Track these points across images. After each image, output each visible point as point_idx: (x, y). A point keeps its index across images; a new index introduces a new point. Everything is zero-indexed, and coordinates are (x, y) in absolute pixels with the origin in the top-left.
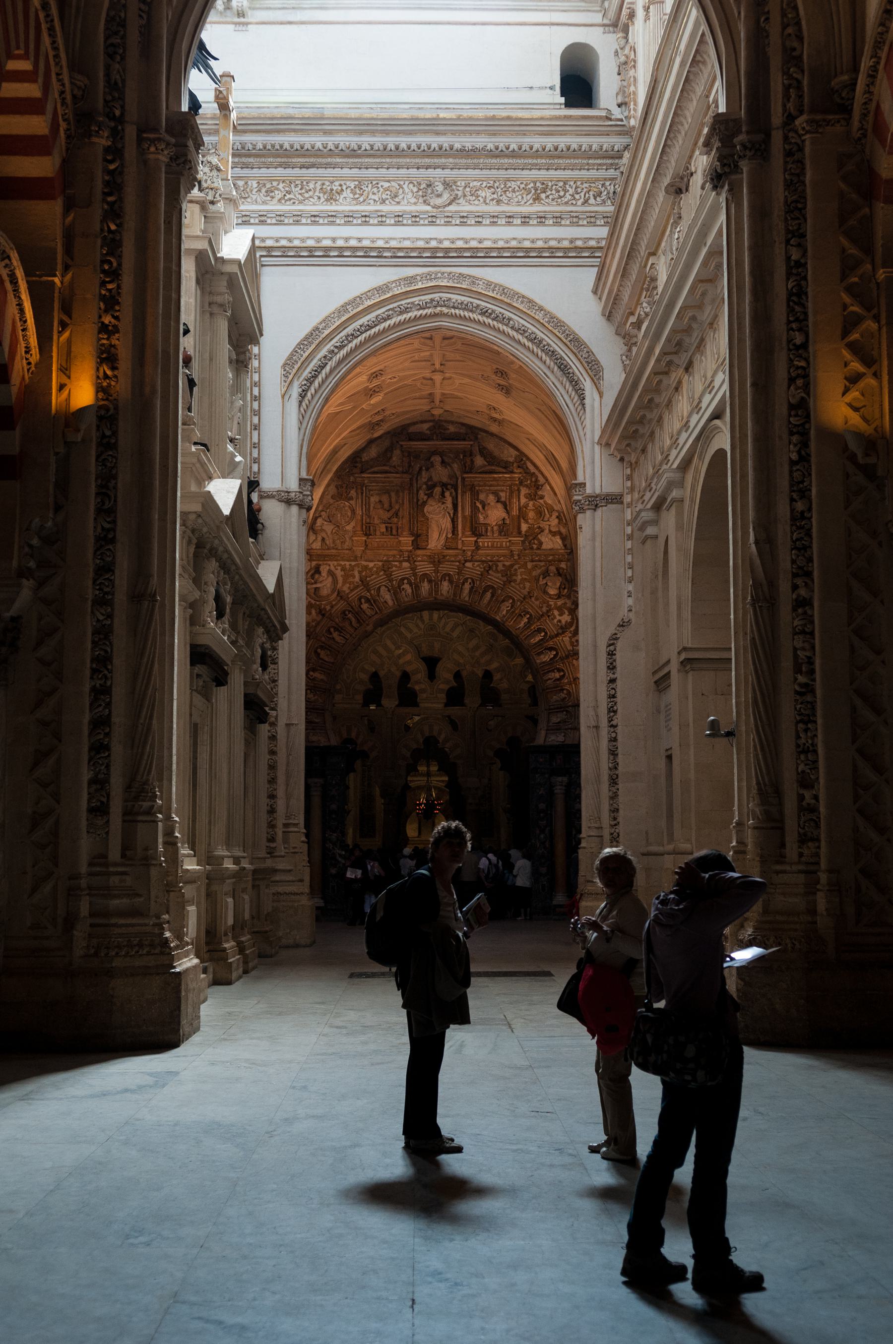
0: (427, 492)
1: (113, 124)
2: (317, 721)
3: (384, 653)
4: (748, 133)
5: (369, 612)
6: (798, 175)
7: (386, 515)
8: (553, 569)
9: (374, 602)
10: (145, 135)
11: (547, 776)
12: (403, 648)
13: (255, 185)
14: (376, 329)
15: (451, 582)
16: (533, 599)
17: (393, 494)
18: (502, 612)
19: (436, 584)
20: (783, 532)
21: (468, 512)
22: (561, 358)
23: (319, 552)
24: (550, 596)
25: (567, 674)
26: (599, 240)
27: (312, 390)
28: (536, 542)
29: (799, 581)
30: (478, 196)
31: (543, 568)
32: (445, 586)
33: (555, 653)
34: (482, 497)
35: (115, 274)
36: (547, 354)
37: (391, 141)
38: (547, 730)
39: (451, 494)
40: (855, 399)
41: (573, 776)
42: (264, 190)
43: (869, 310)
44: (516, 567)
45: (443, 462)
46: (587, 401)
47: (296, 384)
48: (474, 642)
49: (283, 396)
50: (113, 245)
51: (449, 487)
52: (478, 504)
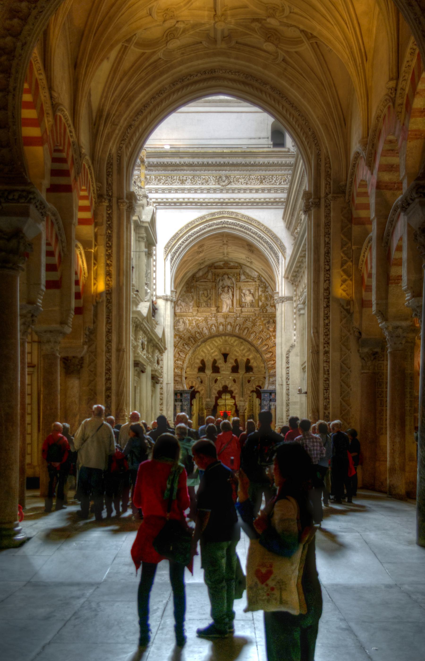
1: (109, 198)
4: (314, 199)
5: (199, 337)
6: (329, 214)
7: (205, 299)
8: (271, 320)
10: (119, 201)
13: (154, 177)
14: (200, 233)
15: (231, 325)
17: (209, 291)
18: (251, 338)
19: (226, 326)
20: (321, 330)
21: (238, 298)
22: (270, 244)
23: (179, 314)
24: (270, 331)
26: (284, 199)
27: (176, 257)
29: (326, 345)
30: (239, 182)
32: (229, 327)
33: (272, 353)
34: (244, 291)
35: (110, 247)
36: (265, 243)
37: (205, 160)
39: (231, 290)
40: (344, 287)
42: (157, 180)
43: (349, 258)
44: (257, 319)
45: (228, 278)
46: (280, 261)
47: (169, 255)
48: (242, 347)
49: (165, 260)
50: (109, 237)
51: (231, 288)
52: (242, 295)
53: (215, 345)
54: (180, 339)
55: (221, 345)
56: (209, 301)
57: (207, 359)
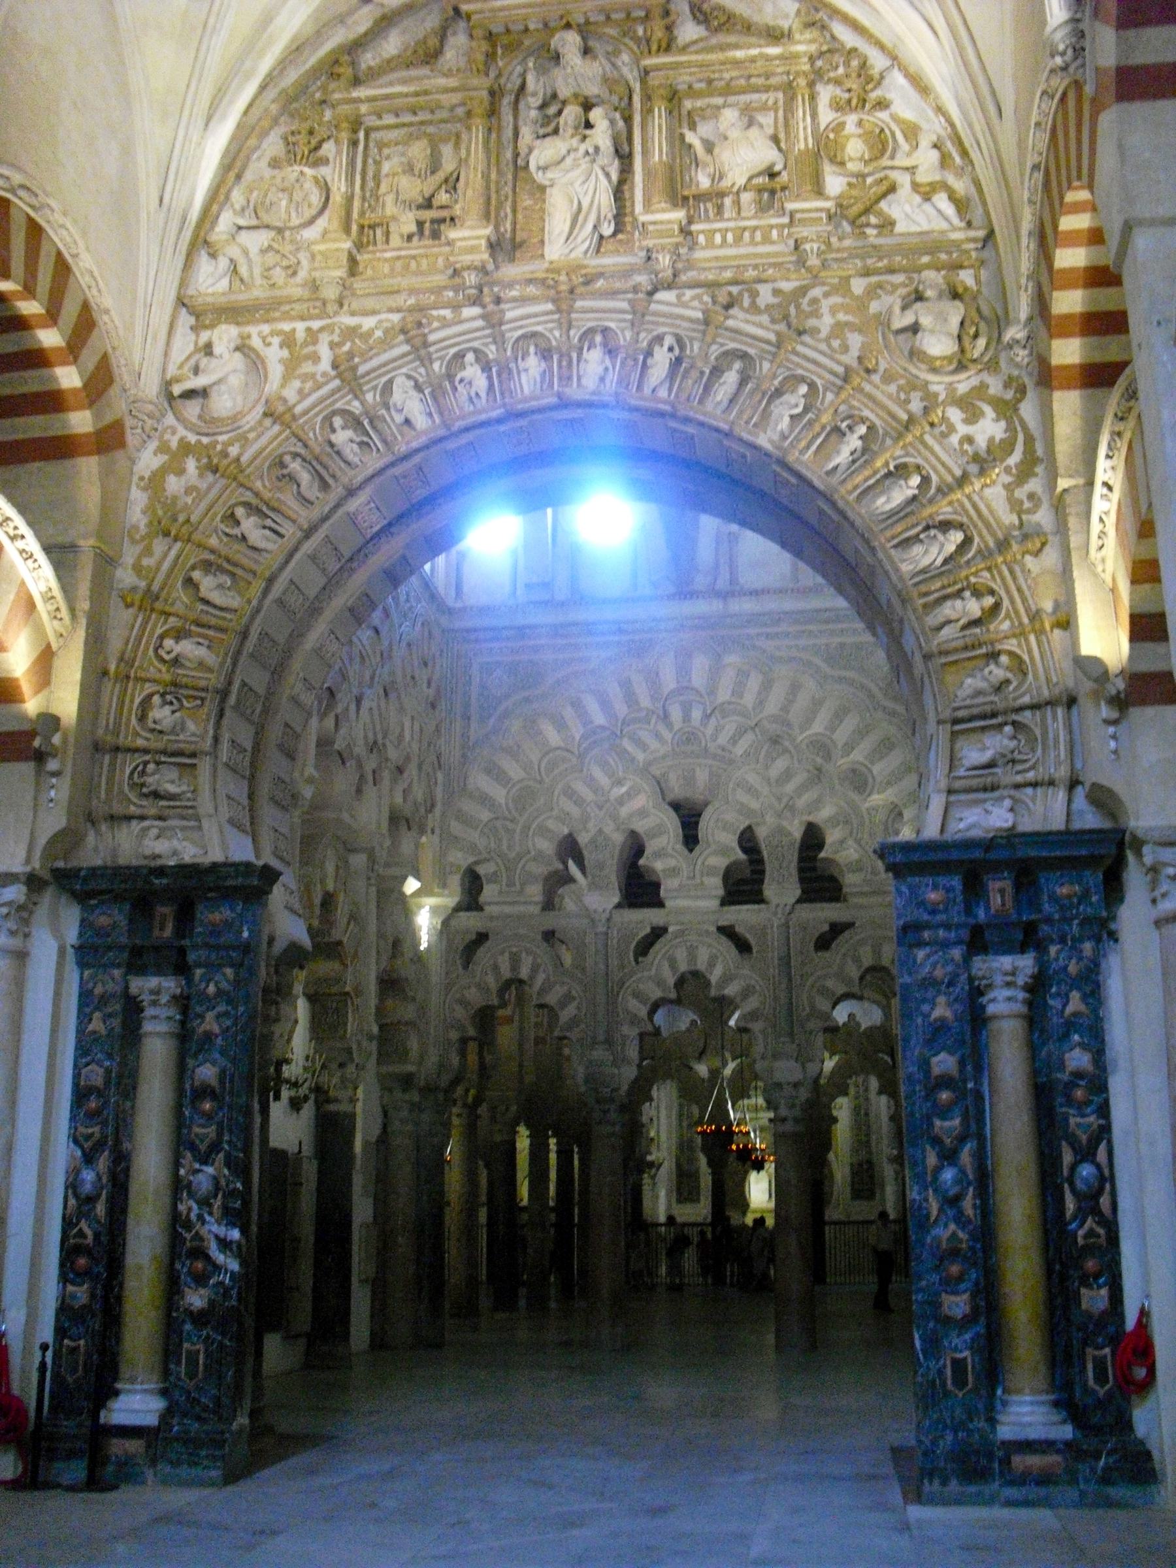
0: (542, 132)
2: (172, 789)
5: (351, 452)
8: (933, 279)
9: (371, 422)
11: (957, 953)
15: (611, 352)
16: (876, 378)
17: (447, 150)
19: (564, 355)
21: (660, 150)
25: (1006, 603)
28: (873, 220)
31: (903, 291)
33: (957, 537)
38: (950, 792)
41: (1053, 950)
44: (817, 292)
45: (586, 51)
48: (780, 764)
52: (690, 137)
53: (633, 760)
54: (210, 478)
55: (664, 757)
56: (443, 197)
57: (593, 831)
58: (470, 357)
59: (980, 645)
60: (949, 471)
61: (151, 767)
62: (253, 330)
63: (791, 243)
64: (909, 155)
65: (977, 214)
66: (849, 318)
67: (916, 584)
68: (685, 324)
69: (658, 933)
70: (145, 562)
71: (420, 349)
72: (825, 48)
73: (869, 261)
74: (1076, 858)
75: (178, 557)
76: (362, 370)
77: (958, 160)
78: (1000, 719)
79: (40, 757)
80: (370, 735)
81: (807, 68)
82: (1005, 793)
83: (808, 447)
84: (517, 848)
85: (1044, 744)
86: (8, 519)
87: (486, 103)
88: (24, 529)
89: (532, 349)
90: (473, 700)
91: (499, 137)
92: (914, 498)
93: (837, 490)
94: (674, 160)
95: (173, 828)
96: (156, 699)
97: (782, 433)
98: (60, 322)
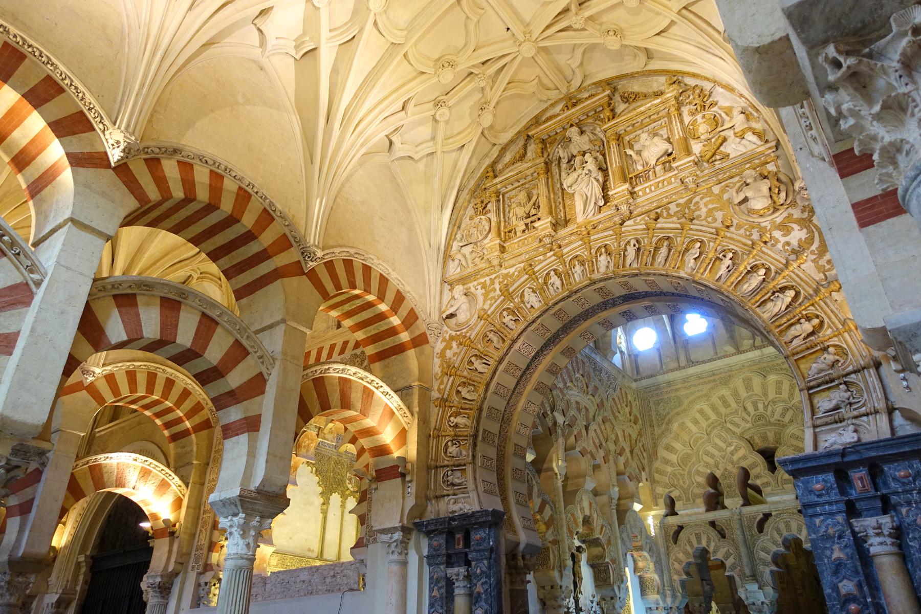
2: (457, 481)
3: (716, 453)
5: (511, 324)
8: (749, 174)
11: (840, 518)
12: (735, 444)
16: (732, 229)
18: (688, 267)
25: (826, 320)
32: (603, 260)
33: (792, 293)
38: (815, 427)
41: (904, 510)
44: (697, 199)
45: (582, 132)
52: (629, 152)
53: (734, 433)
55: (749, 429)
56: (533, 212)
58: (552, 273)
59: (816, 345)
60: (780, 262)
61: (450, 472)
62: (471, 285)
63: (678, 181)
64: (730, 121)
65: (770, 137)
66: (715, 205)
67: (772, 323)
68: (640, 232)
69: (767, 516)
70: (442, 387)
71: (533, 275)
72: (681, 91)
73: (720, 177)
74: (905, 452)
75: (453, 383)
76: (511, 290)
77: (756, 114)
78: (836, 382)
79: (403, 475)
80: (597, 441)
81: (674, 102)
82: (849, 422)
83: (705, 271)
84: (687, 483)
85: (869, 392)
86: (372, 381)
87: (544, 168)
88: (381, 383)
89: (576, 263)
90: (654, 418)
91: (552, 180)
92: (764, 280)
93: (722, 288)
94: (623, 163)
95: (458, 498)
96: (450, 443)
97: (692, 268)
98: (385, 300)
